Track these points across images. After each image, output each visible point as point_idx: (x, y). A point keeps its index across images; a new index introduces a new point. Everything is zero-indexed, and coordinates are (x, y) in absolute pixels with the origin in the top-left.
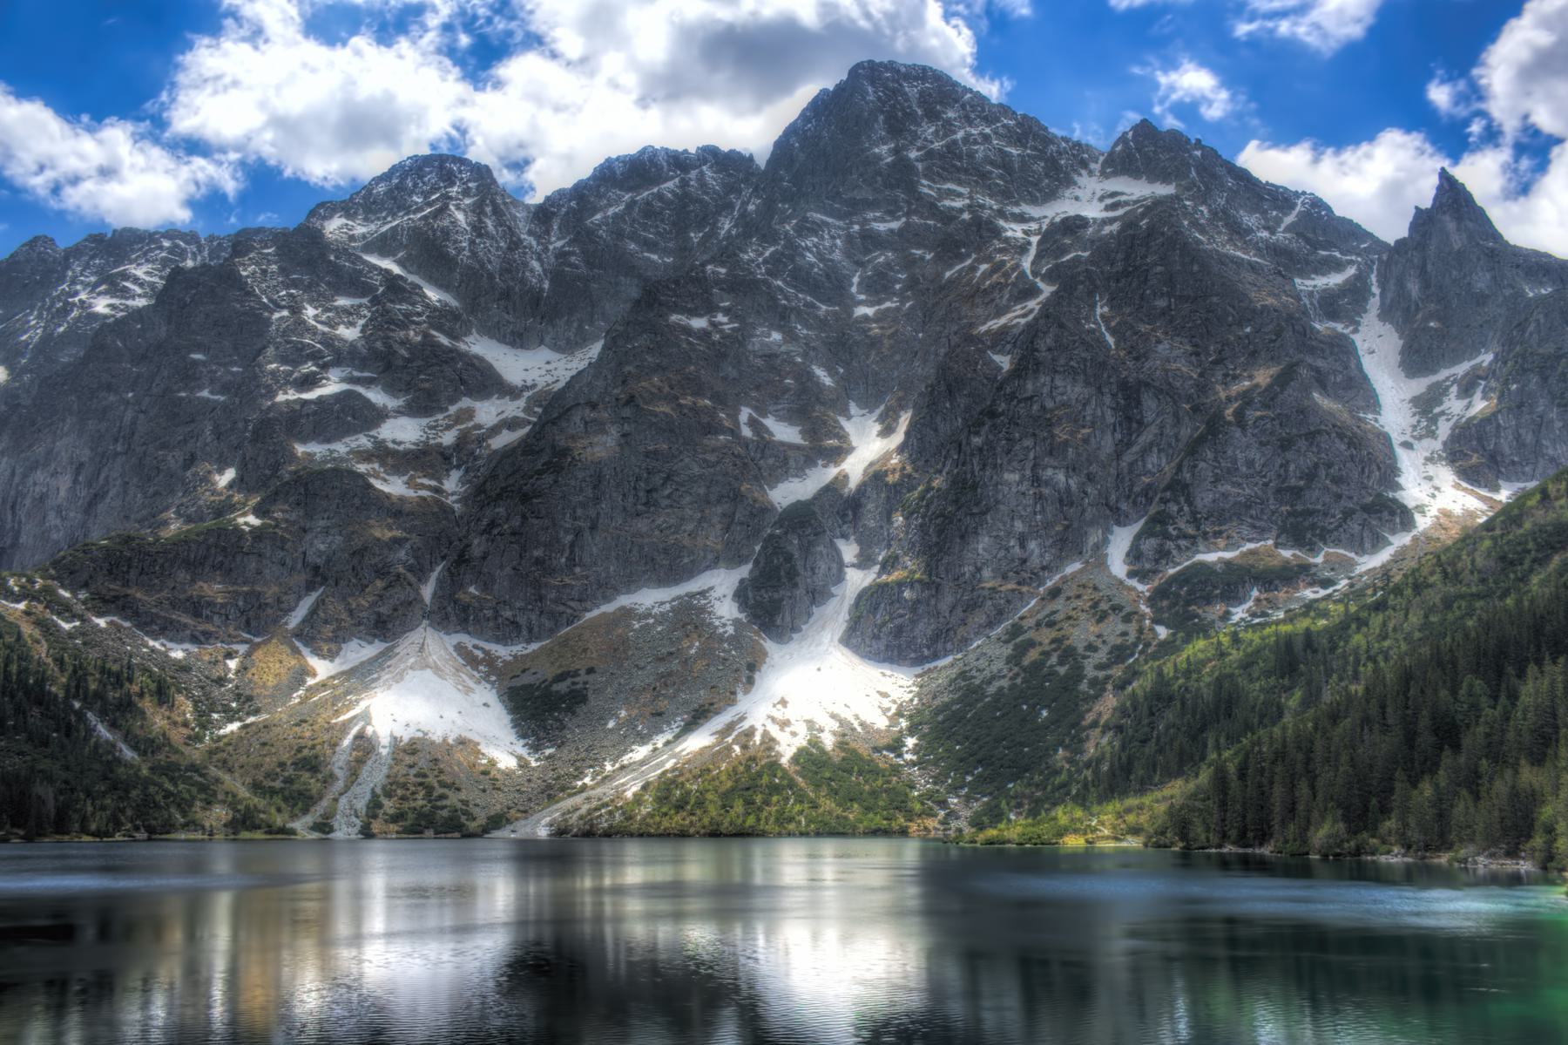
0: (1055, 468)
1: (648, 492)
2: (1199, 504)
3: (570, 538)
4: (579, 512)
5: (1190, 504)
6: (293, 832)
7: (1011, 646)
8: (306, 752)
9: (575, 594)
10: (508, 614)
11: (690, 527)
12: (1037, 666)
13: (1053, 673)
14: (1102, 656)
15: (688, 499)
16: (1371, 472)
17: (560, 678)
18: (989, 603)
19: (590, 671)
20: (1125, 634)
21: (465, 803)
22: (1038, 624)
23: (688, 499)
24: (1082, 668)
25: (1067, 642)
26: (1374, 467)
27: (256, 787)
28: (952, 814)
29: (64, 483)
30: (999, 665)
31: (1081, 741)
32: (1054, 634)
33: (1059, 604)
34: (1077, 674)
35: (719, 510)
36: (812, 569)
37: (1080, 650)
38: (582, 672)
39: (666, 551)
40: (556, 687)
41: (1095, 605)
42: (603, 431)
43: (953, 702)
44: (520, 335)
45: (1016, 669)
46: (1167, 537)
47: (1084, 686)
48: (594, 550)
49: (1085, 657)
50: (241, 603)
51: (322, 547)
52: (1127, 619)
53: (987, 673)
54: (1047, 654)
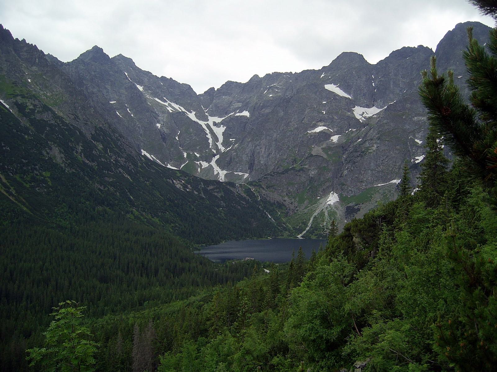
3: (363, 172)
6: (298, 237)
8: (304, 221)
10: (350, 189)
11: (391, 169)
27: (294, 228)
29: (263, 150)
42: (373, 146)
48: (369, 175)
50: (296, 186)
51: (313, 173)
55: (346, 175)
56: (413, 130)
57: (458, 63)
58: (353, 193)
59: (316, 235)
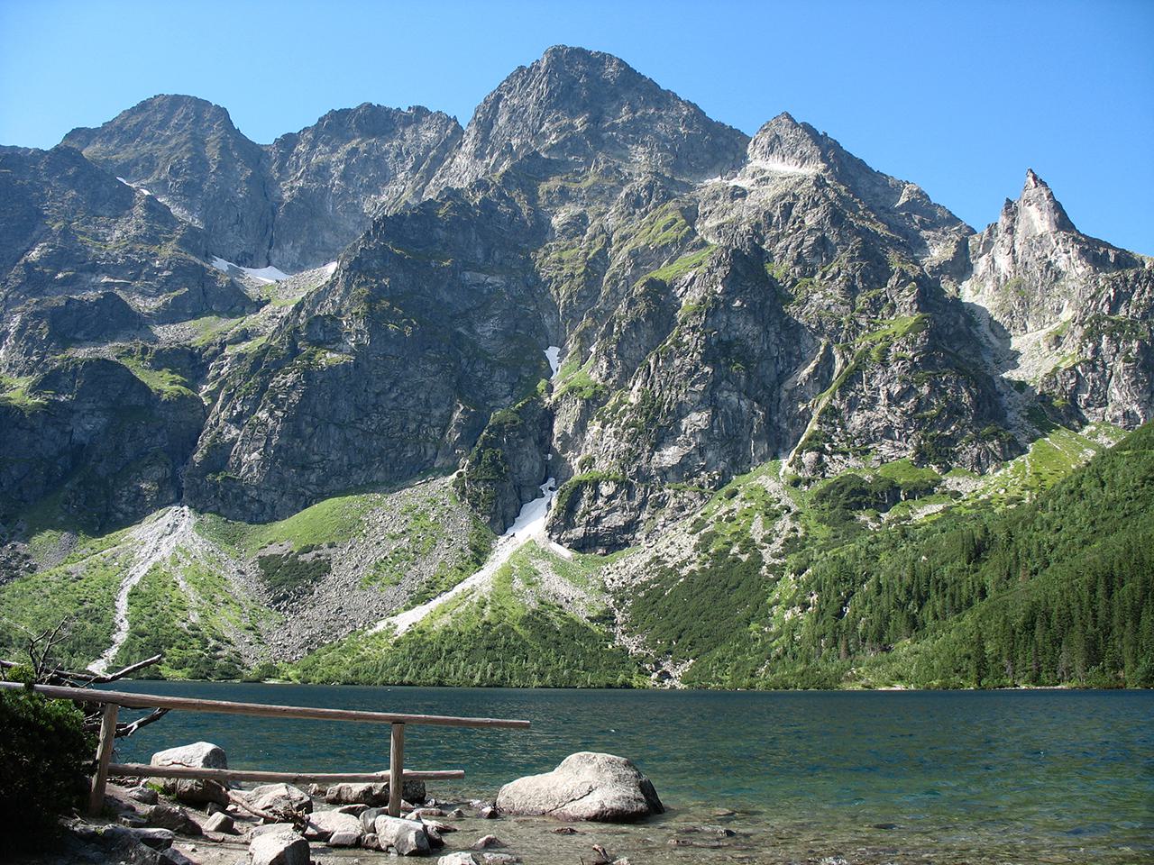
0: (729, 391)
1: (378, 395)
2: (850, 426)
3: (310, 430)
4: (319, 408)
5: (843, 427)
7: (697, 537)
8: (87, 605)
9: (313, 478)
12: (722, 554)
13: (736, 560)
14: (777, 546)
15: (411, 402)
16: (984, 407)
17: (307, 550)
18: (673, 501)
19: (331, 546)
20: (795, 530)
21: (238, 654)
22: (719, 519)
23: (411, 402)
24: (761, 556)
25: (746, 536)
26: (987, 404)
28: (666, 675)
30: (687, 552)
31: (767, 616)
32: (730, 528)
33: (736, 504)
34: (757, 561)
35: (437, 413)
36: (519, 467)
37: (758, 542)
38: (325, 545)
39: (393, 446)
40: (301, 558)
41: (768, 504)
43: (651, 581)
44: (251, 257)
45: (703, 555)
46: (827, 453)
47: (764, 570)
49: (763, 548)
52: (796, 516)
53: (678, 559)
54: (730, 544)
55: (233, 442)
56: (463, 311)
57: (569, 143)
58: (268, 510)
59: (180, 666)
